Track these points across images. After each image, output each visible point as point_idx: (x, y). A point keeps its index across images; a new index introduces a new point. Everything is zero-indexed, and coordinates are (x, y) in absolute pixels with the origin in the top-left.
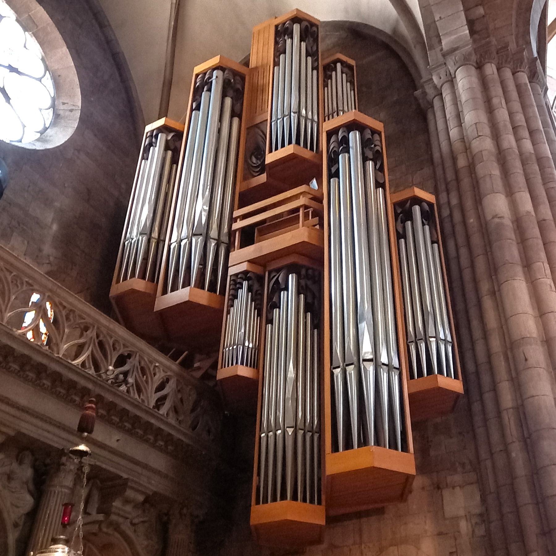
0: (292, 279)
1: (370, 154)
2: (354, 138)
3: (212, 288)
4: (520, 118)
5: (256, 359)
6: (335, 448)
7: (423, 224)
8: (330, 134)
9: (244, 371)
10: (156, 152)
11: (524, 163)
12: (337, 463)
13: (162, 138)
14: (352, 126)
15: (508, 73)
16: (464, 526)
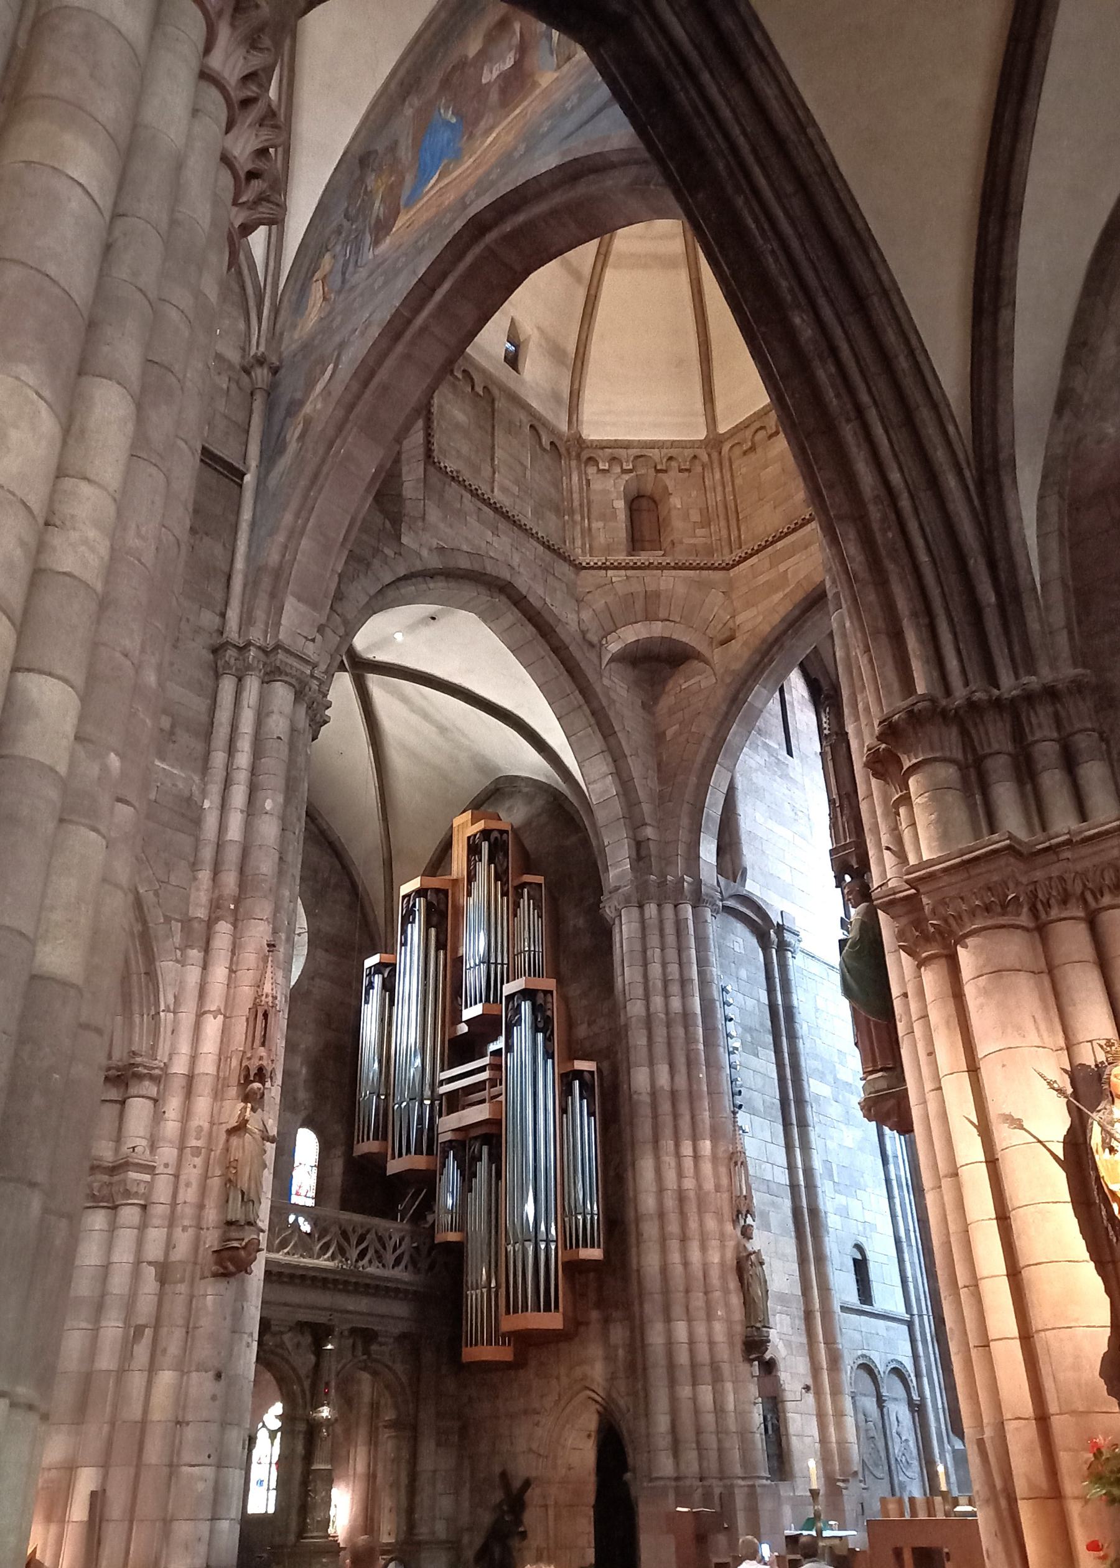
0: (485, 1149)
1: (541, 1025)
2: (526, 1007)
3: (430, 1152)
4: (673, 969)
5: (461, 1227)
6: (508, 1312)
7: (582, 1098)
8: (510, 998)
9: (453, 1237)
10: (375, 994)
11: (668, 1026)
12: (510, 1323)
13: (377, 980)
14: (527, 994)
15: (669, 910)
16: (621, 1352)
